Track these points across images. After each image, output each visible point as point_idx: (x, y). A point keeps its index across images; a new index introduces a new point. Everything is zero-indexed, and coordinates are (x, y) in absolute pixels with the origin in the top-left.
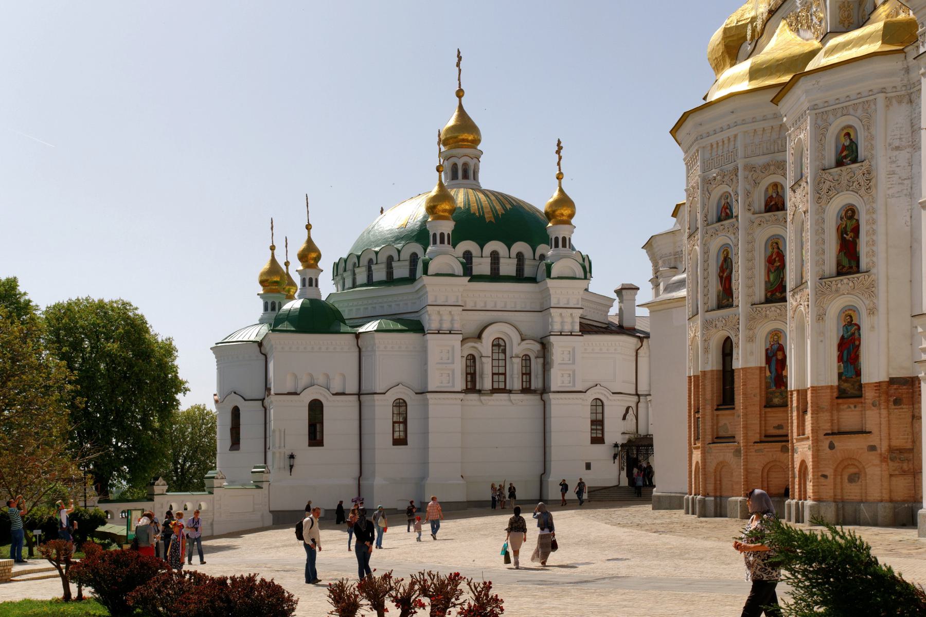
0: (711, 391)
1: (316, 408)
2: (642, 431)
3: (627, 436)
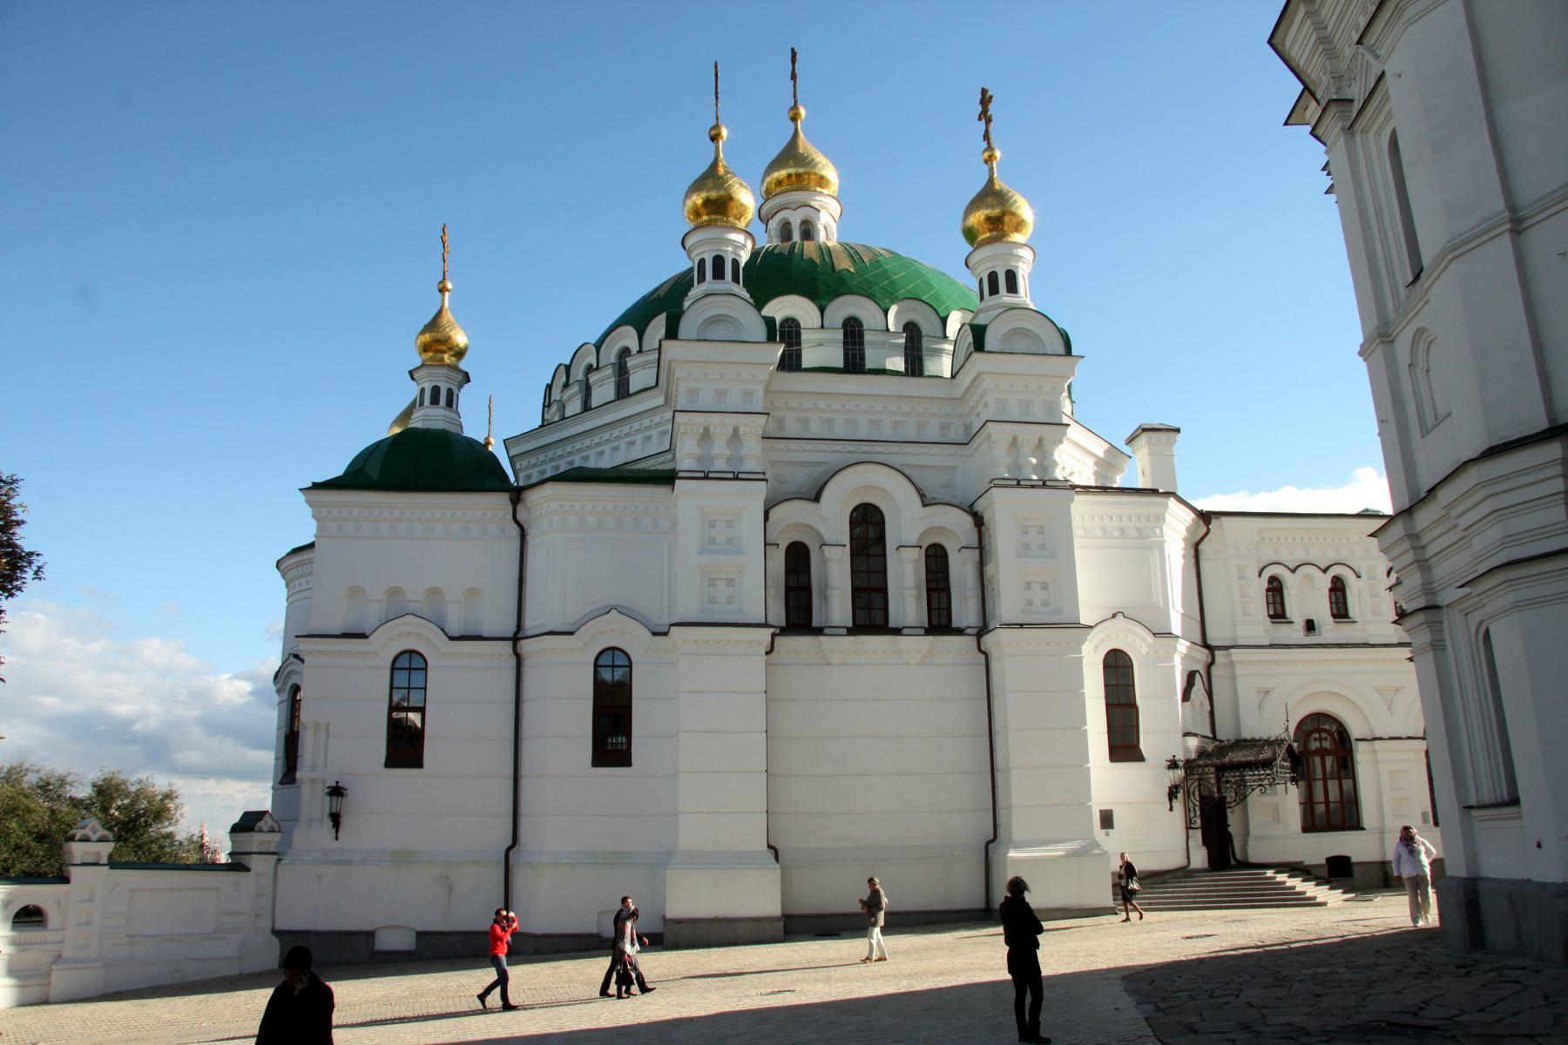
2: (1225, 733)
3: (1193, 743)
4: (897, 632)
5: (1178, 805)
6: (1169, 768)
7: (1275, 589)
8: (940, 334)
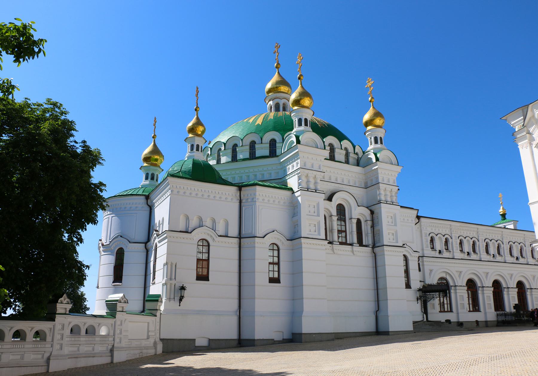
3: (422, 284)
4: (351, 245)
5: (419, 301)
6: (418, 291)
7: (432, 240)
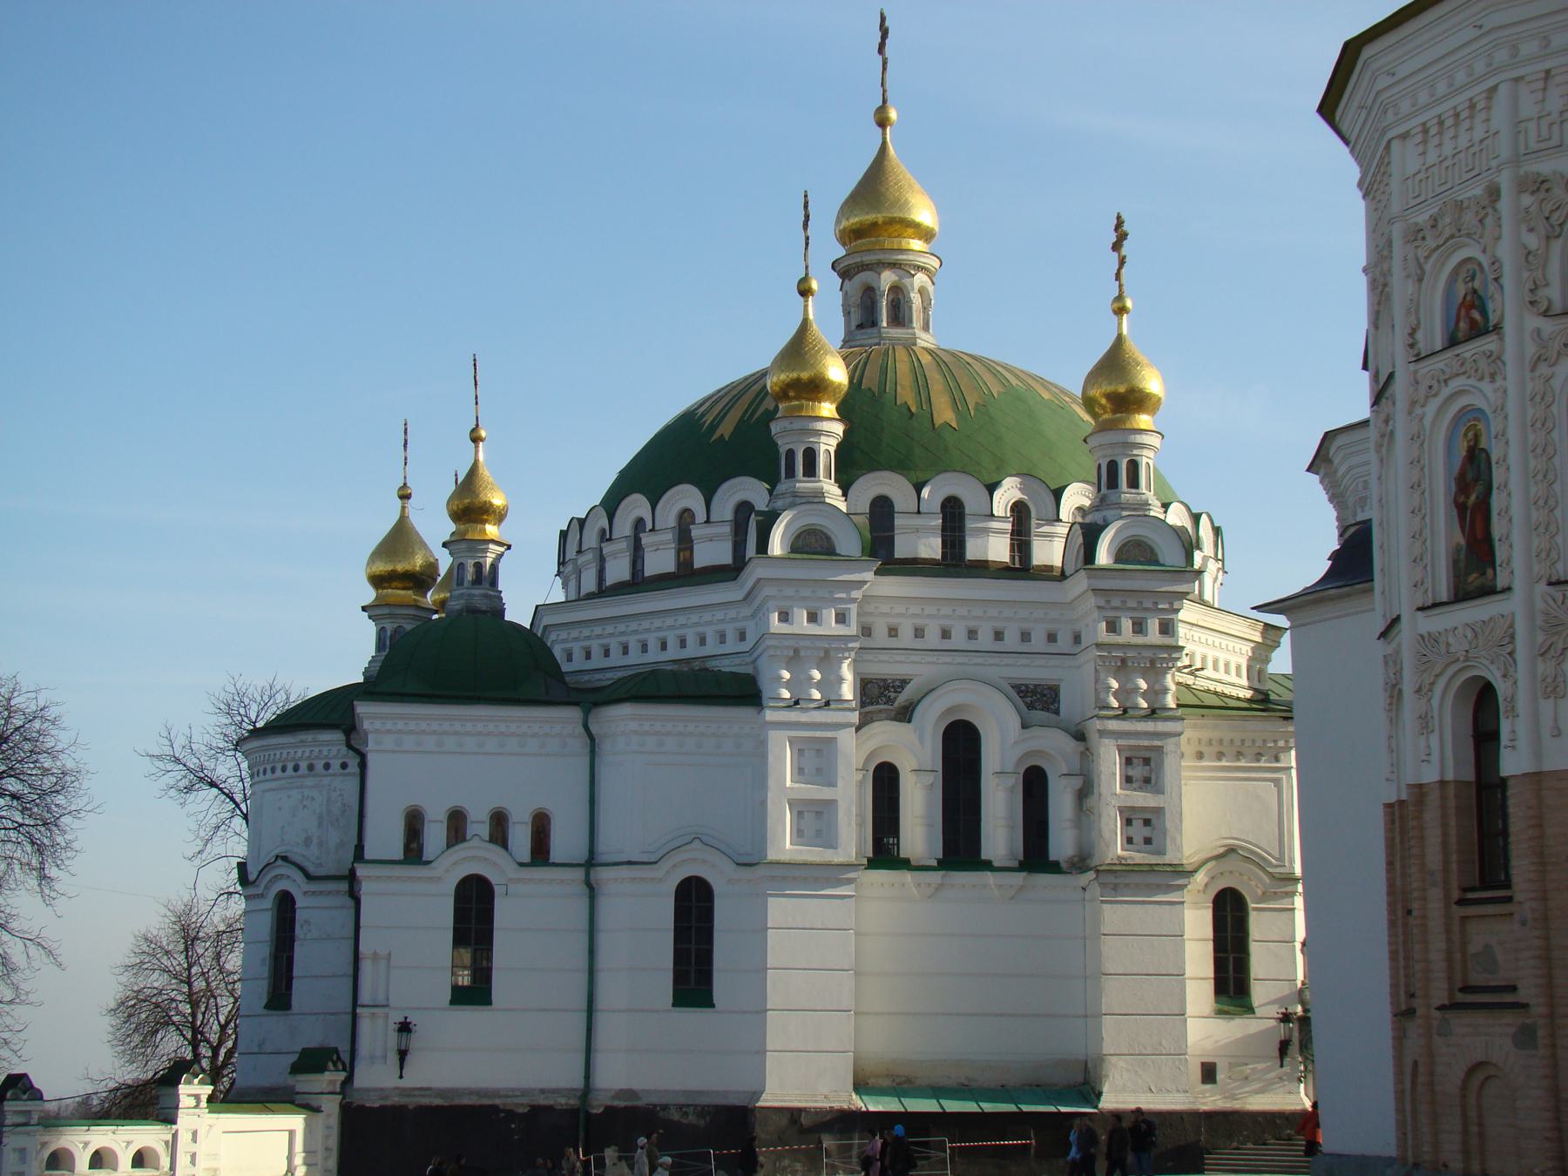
0: (1437, 840)
1: (474, 909)
4: (987, 866)
8: (1052, 515)
